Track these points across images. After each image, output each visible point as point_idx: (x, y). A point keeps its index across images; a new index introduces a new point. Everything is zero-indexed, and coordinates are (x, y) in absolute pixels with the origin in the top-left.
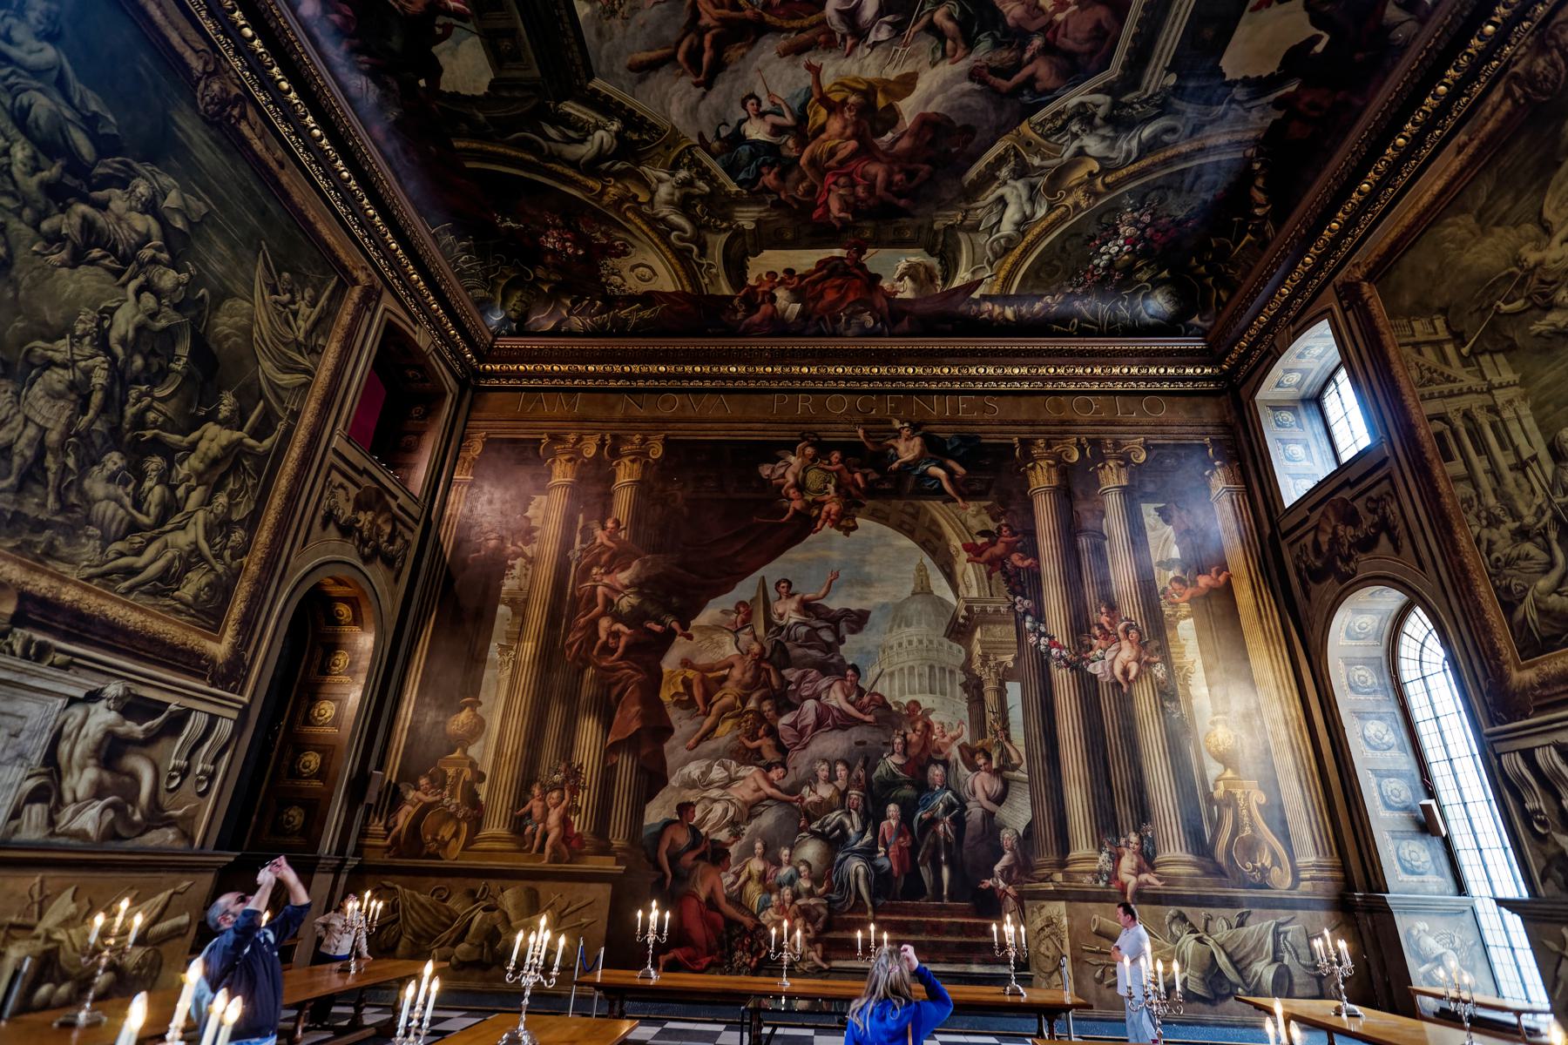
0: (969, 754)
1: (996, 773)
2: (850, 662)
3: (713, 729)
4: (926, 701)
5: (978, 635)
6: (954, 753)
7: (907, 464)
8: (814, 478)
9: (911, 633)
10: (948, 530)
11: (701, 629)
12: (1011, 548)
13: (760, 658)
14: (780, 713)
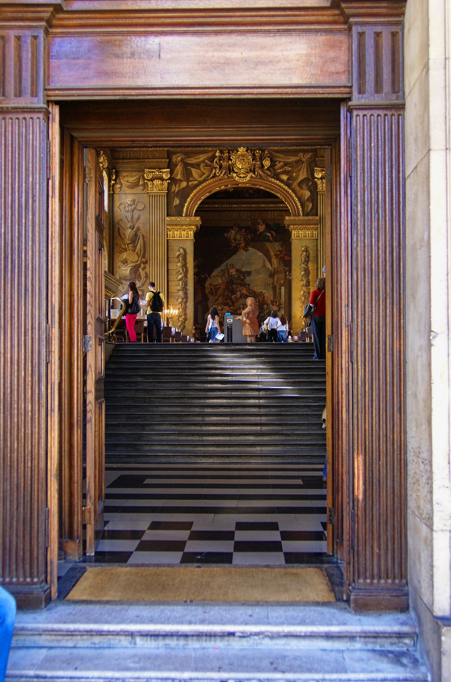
0: (272, 302)
1: (278, 306)
3: (218, 298)
4: (264, 291)
6: (269, 302)
7: (261, 232)
8: (238, 237)
9: (261, 276)
11: (213, 277)
13: (227, 283)
14: (232, 295)
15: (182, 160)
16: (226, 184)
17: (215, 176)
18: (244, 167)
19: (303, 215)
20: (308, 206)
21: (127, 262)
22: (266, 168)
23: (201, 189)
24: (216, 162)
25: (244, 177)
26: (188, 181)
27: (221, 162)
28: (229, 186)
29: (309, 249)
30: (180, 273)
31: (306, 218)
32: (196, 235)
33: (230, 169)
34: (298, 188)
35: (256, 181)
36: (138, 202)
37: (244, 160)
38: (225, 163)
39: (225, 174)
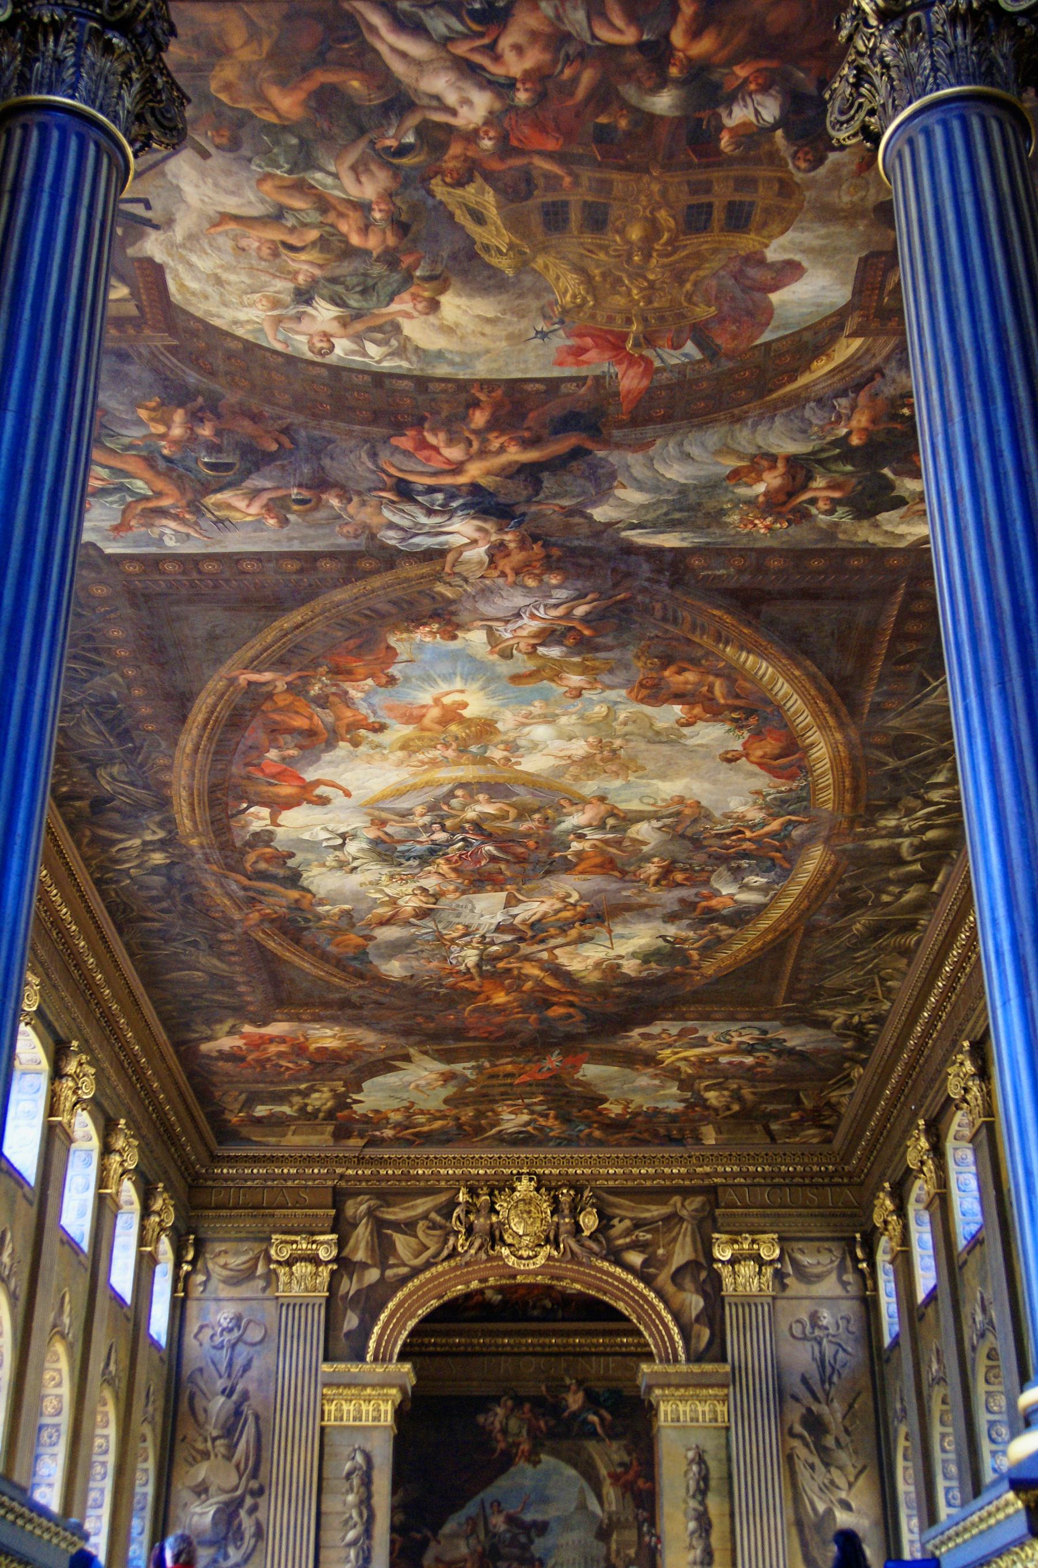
2: (537, 1555)
5: (614, 1536)
8: (513, 1424)
9: (574, 1537)
10: (599, 1463)
11: (445, 1536)
12: (638, 1476)
13: (482, 1556)
15: (370, 1213)
16: (482, 1274)
17: (453, 1254)
18: (530, 1230)
19: (688, 1360)
20: (699, 1336)
21: (206, 1490)
22: (587, 1233)
23: (418, 1288)
24: (458, 1217)
25: (529, 1258)
26: (384, 1266)
27: (472, 1217)
28: (492, 1281)
29: (707, 1458)
30: (351, 1523)
31: (696, 1368)
32: (399, 1413)
33: (495, 1237)
34: (670, 1289)
35: (560, 1267)
36: (249, 1322)
37: (529, 1212)
38: (482, 1220)
39: (480, 1248)
